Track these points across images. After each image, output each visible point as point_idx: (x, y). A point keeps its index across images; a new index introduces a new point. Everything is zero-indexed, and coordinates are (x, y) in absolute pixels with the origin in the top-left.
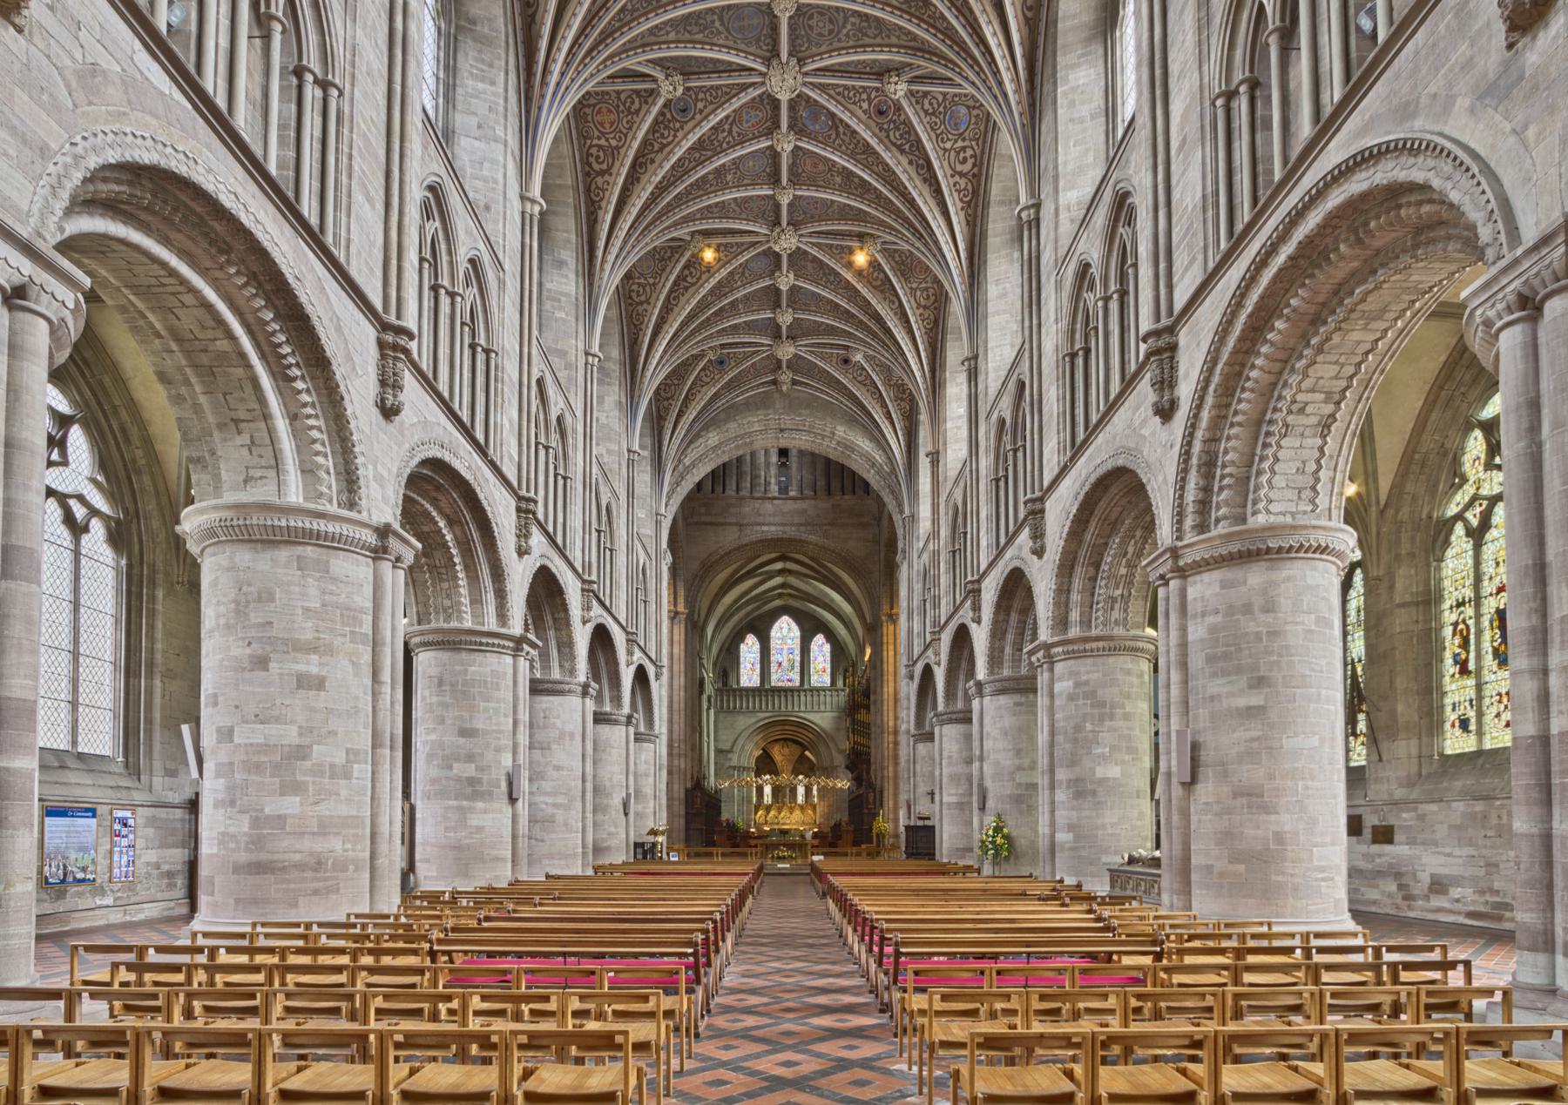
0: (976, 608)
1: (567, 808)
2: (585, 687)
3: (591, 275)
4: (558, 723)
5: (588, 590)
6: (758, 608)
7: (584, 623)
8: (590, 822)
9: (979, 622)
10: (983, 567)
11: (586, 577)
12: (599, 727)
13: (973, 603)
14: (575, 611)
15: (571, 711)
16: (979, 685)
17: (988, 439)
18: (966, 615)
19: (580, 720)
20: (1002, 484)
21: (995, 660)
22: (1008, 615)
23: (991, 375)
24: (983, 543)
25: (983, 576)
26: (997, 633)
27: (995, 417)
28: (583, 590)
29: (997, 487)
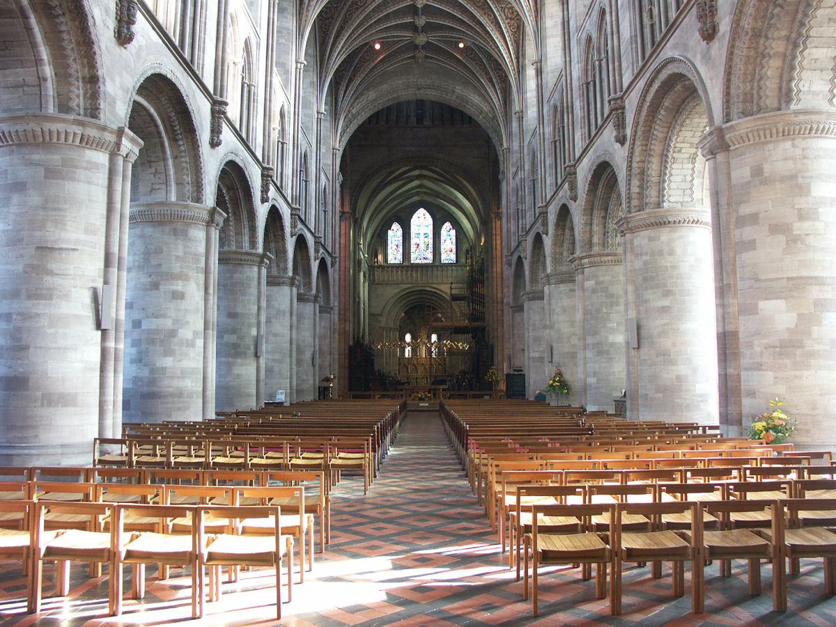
0: (545, 224)
1: (280, 362)
2: (293, 279)
3: (300, 19)
4: (276, 304)
5: (294, 214)
6: (402, 202)
7: (292, 237)
8: (294, 371)
9: (547, 234)
10: (548, 198)
11: (294, 206)
12: (302, 305)
13: (543, 221)
14: (288, 229)
15: (284, 296)
16: (548, 276)
17: (549, 115)
18: (538, 228)
19: (289, 302)
20: (558, 144)
21: (556, 261)
22: (564, 230)
23: (550, 75)
24: (548, 182)
25: (548, 204)
26: (558, 242)
27: (552, 102)
28: (291, 214)
29: (555, 146)
